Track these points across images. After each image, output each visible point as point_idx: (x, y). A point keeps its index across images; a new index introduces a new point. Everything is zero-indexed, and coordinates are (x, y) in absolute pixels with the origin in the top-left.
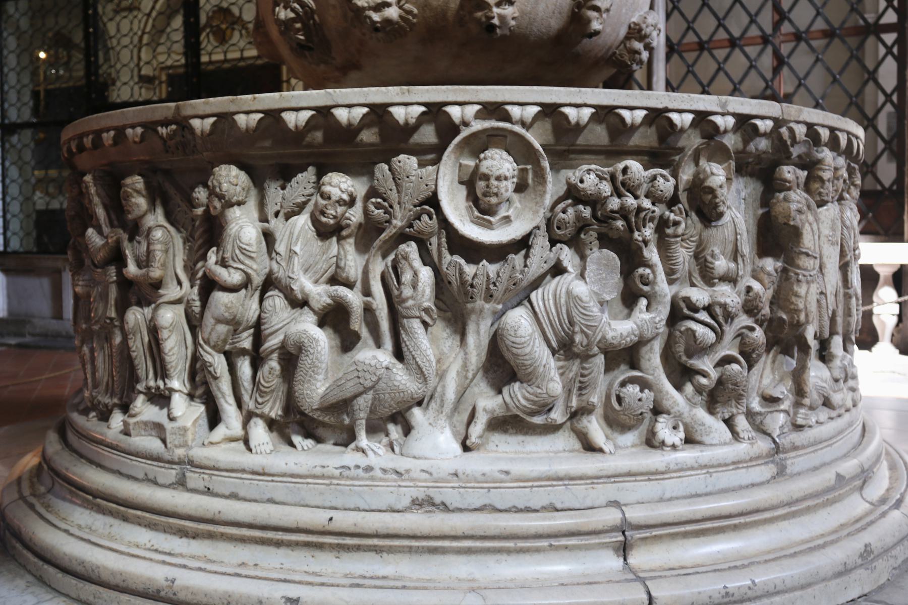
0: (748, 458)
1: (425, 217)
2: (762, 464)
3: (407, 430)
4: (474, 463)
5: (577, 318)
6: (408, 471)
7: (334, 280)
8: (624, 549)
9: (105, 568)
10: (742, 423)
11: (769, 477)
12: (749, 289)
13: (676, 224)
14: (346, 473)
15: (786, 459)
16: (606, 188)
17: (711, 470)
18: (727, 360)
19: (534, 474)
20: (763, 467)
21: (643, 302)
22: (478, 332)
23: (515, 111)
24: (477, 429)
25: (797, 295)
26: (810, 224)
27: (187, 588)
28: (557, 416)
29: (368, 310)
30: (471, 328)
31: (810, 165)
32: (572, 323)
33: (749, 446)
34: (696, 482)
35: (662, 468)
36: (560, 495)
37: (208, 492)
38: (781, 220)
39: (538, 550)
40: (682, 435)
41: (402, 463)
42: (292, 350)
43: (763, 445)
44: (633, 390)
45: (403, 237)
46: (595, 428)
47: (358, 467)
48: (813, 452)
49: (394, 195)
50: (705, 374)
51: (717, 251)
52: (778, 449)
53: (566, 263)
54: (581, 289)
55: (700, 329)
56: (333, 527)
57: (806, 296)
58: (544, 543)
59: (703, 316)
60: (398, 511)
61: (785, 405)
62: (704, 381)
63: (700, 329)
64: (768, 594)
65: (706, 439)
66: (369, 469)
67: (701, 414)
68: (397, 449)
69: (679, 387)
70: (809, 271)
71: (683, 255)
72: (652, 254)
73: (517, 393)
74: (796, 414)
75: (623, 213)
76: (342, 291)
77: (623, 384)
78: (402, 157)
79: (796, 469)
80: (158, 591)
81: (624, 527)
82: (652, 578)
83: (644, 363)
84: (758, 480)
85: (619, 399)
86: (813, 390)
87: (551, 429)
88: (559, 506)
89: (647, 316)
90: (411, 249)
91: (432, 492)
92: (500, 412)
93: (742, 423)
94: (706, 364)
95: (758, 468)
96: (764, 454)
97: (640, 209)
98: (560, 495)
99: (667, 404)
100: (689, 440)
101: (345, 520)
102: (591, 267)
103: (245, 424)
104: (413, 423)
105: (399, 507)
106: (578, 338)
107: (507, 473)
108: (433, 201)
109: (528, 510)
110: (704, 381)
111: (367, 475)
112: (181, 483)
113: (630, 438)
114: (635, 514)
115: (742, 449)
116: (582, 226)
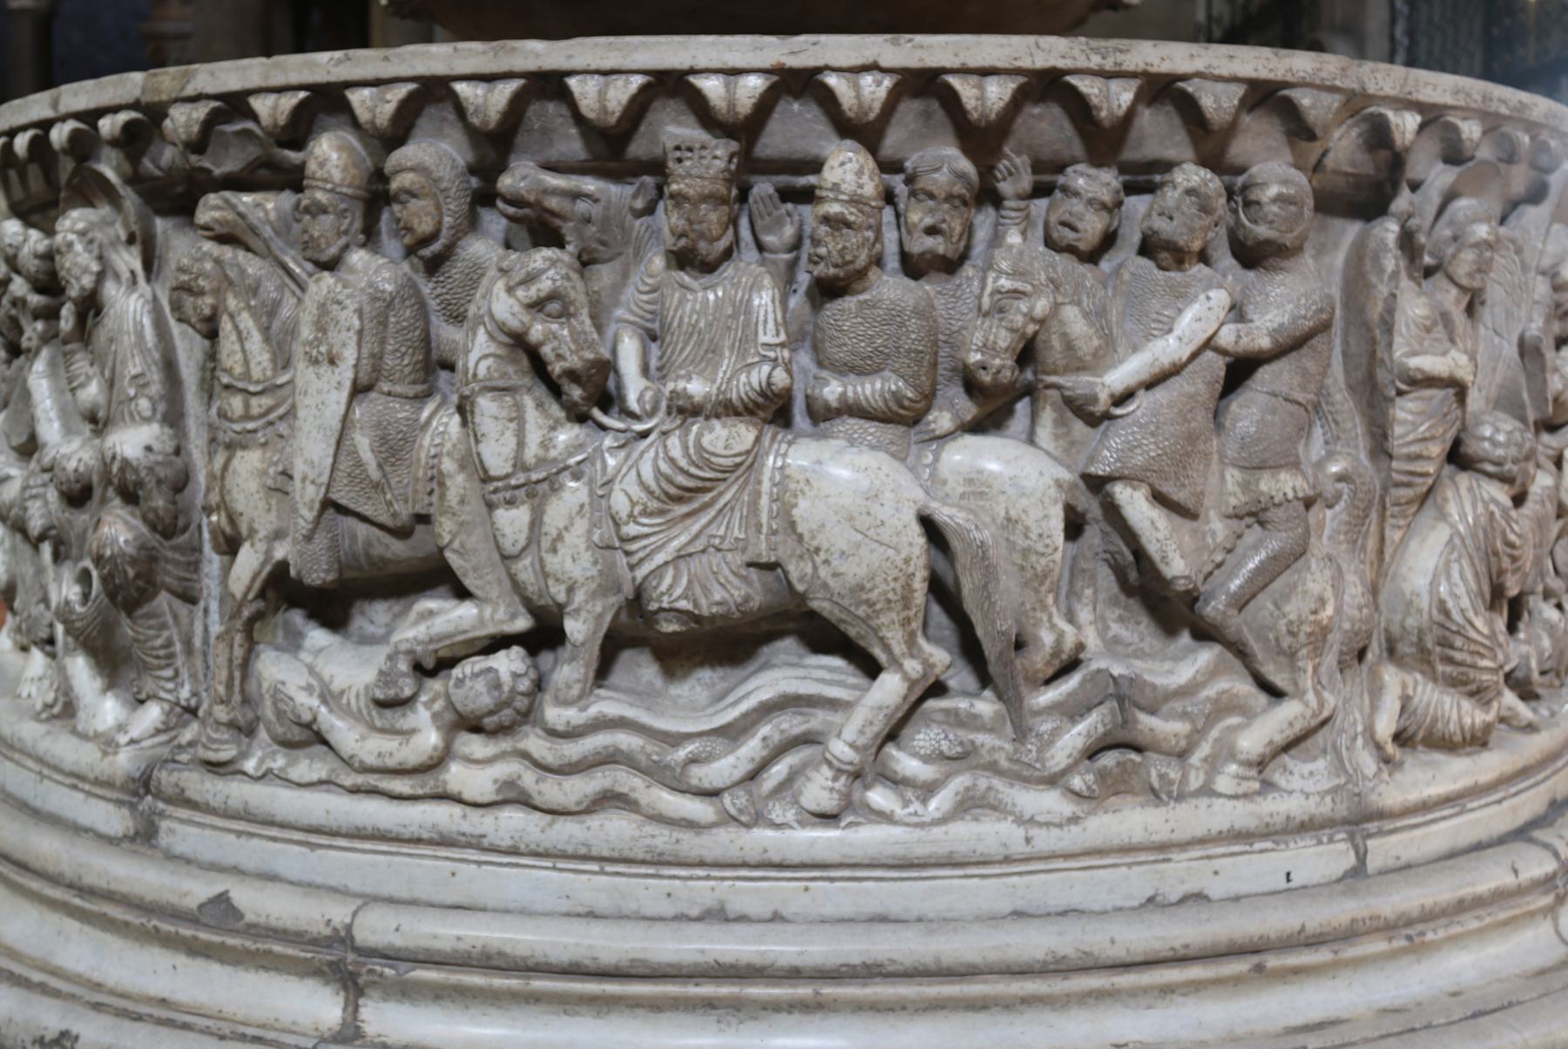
0: (91, 776)
2: (109, 800)
11: (120, 834)
15: (162, 814)
17: (46, 772)
20: (111, 807)
26: (232, 317)
33: (99, 754)
48: (239, 834)
57: (223, 477)
70: (231, 420)
79: (180, 848)
84: (103, 828)
86: (267, 696)
95: (102, 804)
96: (118, 783)
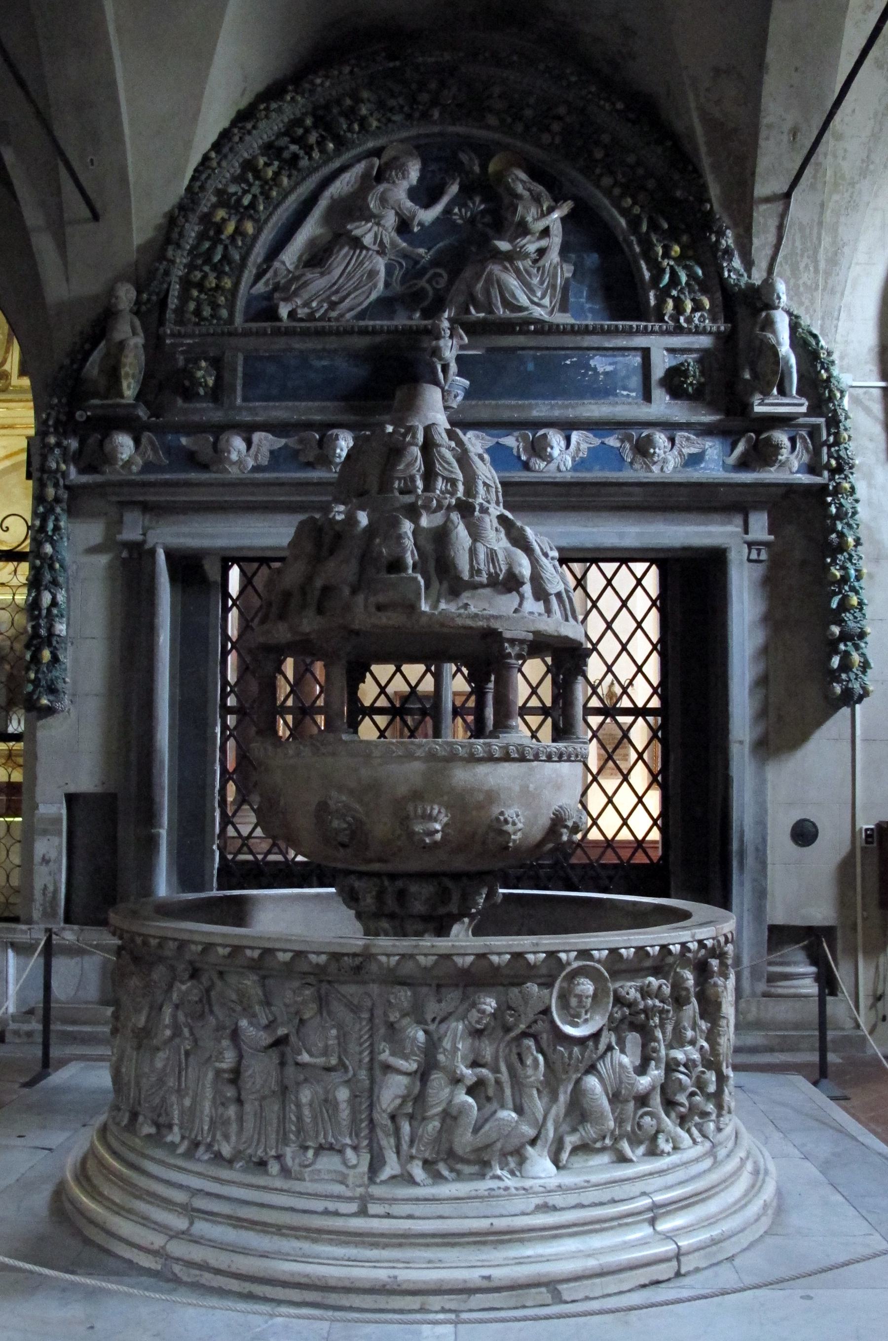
1: (540, 1023)
3: (522, 1161)
4: (567, 1179)
5: (625, 1079)
6: (531, 1187)
7: (475, 1064)
8: (652, 1222)
9: (332, 1277)
10: (694, 1130)
12: (702, 1047)
13: (668, 1011)
14: (493, 1193)
16: (638, 995)
18: (693, 1094)
19: (603, 1181)
21: (653, 1063)
22: (566, 1092)
23: (595, 953)
24: (565, 1156)
25: (719, 1044)
27: (409, 1281)
28: (608, 1142)
29: (498, 1082)
30: (561, 1090)
31: (721, 956)
32: (621, 1082)
34: (681, 1174)
35: (665, 1167)
36: (617, 1192)
37: (388, 1216)
38: (713, 999)
39: (612, 1228)
40: (671, 1145)
41: (528, 1183)
42: (454, 1112)
43: (708, 1145)
44: (647, 1119)
45: (525, 1035)
46: (625, 1146)
47: (499, 1188)
49: (521, 1009)
50: (682, 1105)
51: (686, 1024)
52: (714, 1146)
53: (614, 1044)
54: (625, 1060)
55: (681, 1076)
56: (493, 1229)
58: (615, 1223)
59: (682, 1069)
60: (527, 1214)
61: (714, 1117)
62: (682, 1109)
63: (681, 1076)
64: (730, 1237)
65: (682, 1146)
66: (507, 1189)
67: (679, 1129)
68: (518, 1173)
69: (668, 1115)
71: (669, 1028)
72: (659, 1034)
73: (590, 1131)
74: (718, 1122)
75: (645, 1011)
76: (484, 1071)
77: (641, 1117)
78: (529, 984)
80: (384, 1286)
81: (655, 1206)
82: (675, 1236)
83: (652, 1102)
85: (640, 1126)
87: (603, 1149)
88: (616, 1199)
89: (656, 1072)
90: (531, 1043)
91: (548, 1200)
92: (578, 1143)
93: (694, 1130)
94: (682, 1098)
97: (654, 1006)
98: (617, 1192)
99: (663, 1126)
100: (675, 1148)
101: (501, 1223)
102: (628, 1046)
103: (403, 1166)
104: (527, 1155)
105: (528, 1211)
106: (623, 1092)
107: (588, 1182)
108: (547, 1011)
109: (601, 1204)
110: (682, 1109)
111: (506, 1193)
112: (363, 1212)
113: (641, 1150)
114: (659, 1198)
115: (699, 1150)
116: (622, 1020)
